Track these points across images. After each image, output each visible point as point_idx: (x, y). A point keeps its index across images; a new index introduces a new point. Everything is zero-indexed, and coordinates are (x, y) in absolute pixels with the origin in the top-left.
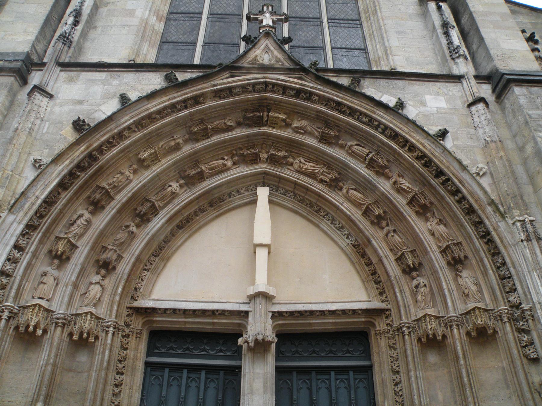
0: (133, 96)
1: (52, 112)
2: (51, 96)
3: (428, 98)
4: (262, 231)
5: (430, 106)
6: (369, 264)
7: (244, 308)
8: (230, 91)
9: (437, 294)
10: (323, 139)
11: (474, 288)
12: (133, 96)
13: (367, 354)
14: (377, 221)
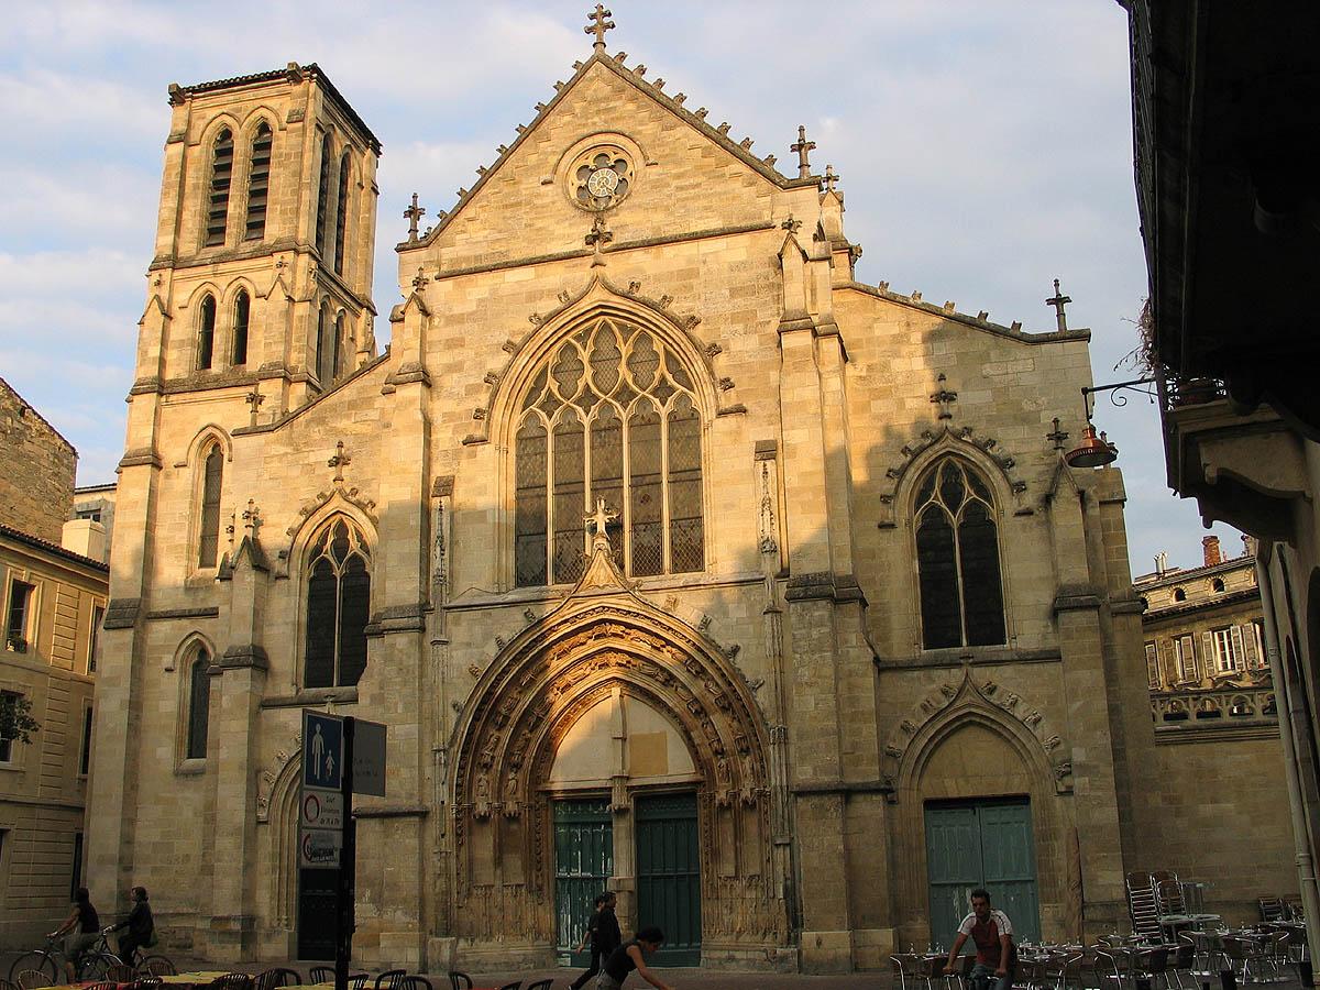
0: (506, 636)
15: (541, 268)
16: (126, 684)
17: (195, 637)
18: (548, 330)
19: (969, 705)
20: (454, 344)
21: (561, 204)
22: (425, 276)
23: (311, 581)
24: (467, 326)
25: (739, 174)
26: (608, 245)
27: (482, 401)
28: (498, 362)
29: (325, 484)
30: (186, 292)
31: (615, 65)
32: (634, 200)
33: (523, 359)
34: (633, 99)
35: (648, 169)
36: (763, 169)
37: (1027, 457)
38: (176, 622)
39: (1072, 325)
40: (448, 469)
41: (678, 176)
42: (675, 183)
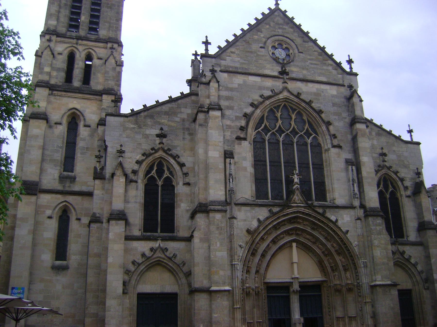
1: (238, 225)
2: (235, 218)
3: (345, 216)
5: (345, 220)
6: (323, 267)
7: (292, 281)
8: (287, 214)
9: (340, 278)
10: (313, 229)
11: (349, 277)
12: (262, 218)
13: (320, 291)
14: (326, 255)
15: (264, 79)
16: (31, 221)
17: (64, 203)
18: (267, 102)
19: (398, 258)
20: (228, 98)
21: (268, 57)
22: (215, 69)
23: (146, 185)
25: (331, 65)
26: (287, 77)
27: (243, 123)
28: (249, 110)
29: (155, 144)
30: (62, 48)
32: (295, 63)
33: (258, 111)
34: (291, 28)
35: (299, 54)
37: (408, 179)
38: (54, 195)
39: (415, 140)
40: (229, 148)
41: (310, 59)
42: (309, 61)
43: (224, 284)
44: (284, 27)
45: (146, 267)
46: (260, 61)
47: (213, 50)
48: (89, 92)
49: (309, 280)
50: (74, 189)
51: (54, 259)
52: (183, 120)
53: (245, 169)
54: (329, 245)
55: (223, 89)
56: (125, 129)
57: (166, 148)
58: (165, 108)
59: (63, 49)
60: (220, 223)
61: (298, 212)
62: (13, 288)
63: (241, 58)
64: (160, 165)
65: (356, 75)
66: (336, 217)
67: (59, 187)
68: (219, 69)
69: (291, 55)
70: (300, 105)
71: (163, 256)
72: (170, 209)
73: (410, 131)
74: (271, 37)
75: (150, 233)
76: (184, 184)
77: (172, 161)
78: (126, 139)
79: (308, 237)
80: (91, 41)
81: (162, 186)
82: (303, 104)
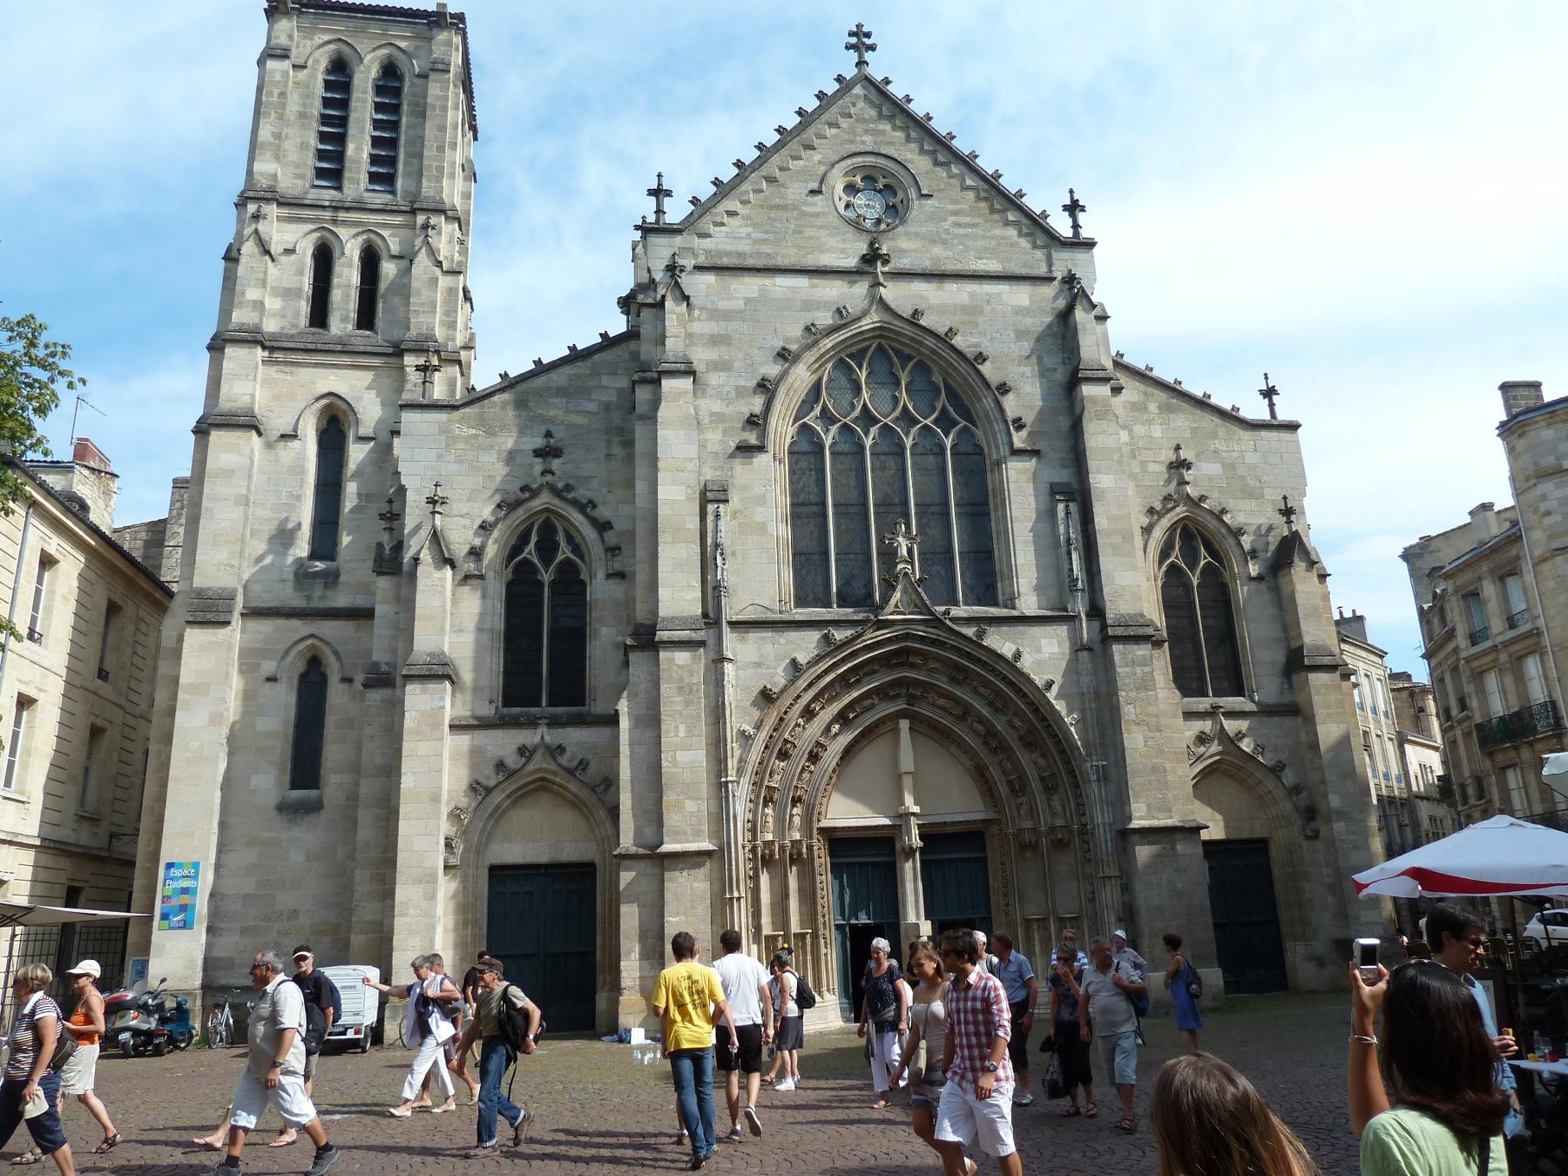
3: (1044, 641)
4: (907, 761)
6: (987, 782)
10: (953, 680)
12: (803, 659)
14: (994, 751)
17: (310, 642)
18: (828, 343)
20: (716, 340)
21: (832, 218)
22: (681, 262)
23: (510, 585)
24: (733, 325)
27: (757, 404)
28: (772, 370)
29: (530, 475)
31: (879, 92)
32: (910, 227)
36: (1036, 225)
38: (281, 623)
39: (1283, 415)
41: (955, 213)
43: (697, 835)
44: (881, 127)
45: (508, 796)
46: (809, 232)
47: (676, 211)
48: (369, 349)
49: (948, 819)
50: (334, 605)
51: (287, 785)
52: (607, 407)
53: (762, 529)
54: (999, 724)
55: (704, 317)
56: (452, 440)
57: (560, 485)
58: (556, 378)
59: (298, 235)
60: (686, 675)
61: (907, 637)
62: (170, 866)
63: (755, 225)
64: (547, 532)
65: (1090, 245)
66: (1015, 642)
67: (298, 602)
68: (693, 262)
69: (899, 206)
70: (920, 343)
71: (553, 767)
72: (572, 642)
73: (1269, 393)
74: (843, 159)
75: (518, 710)
76: (609, 576)
77: (577, 518)
78: (454, 467)
79: (941, 702)
80: (372, 211)
81: (552, 584)
82: (930, 342)
